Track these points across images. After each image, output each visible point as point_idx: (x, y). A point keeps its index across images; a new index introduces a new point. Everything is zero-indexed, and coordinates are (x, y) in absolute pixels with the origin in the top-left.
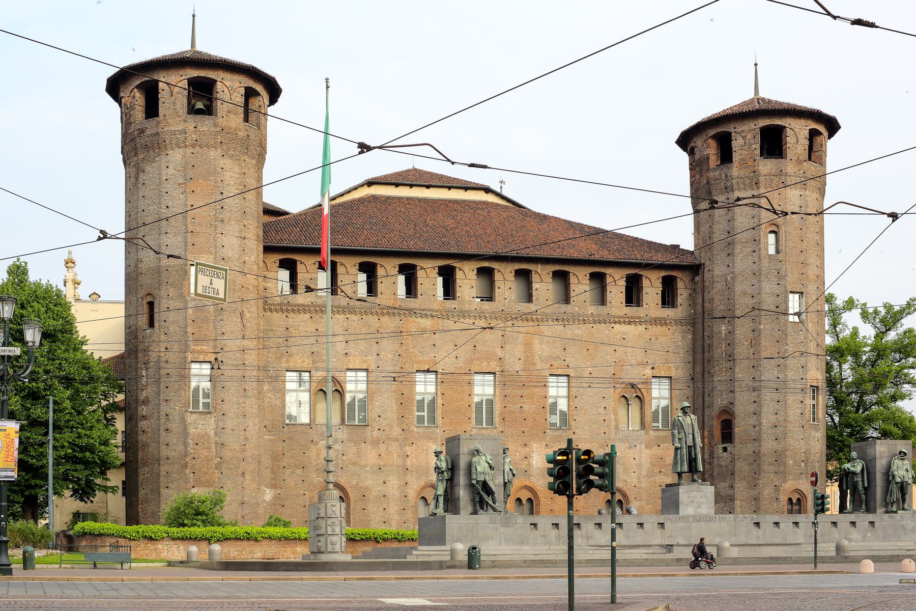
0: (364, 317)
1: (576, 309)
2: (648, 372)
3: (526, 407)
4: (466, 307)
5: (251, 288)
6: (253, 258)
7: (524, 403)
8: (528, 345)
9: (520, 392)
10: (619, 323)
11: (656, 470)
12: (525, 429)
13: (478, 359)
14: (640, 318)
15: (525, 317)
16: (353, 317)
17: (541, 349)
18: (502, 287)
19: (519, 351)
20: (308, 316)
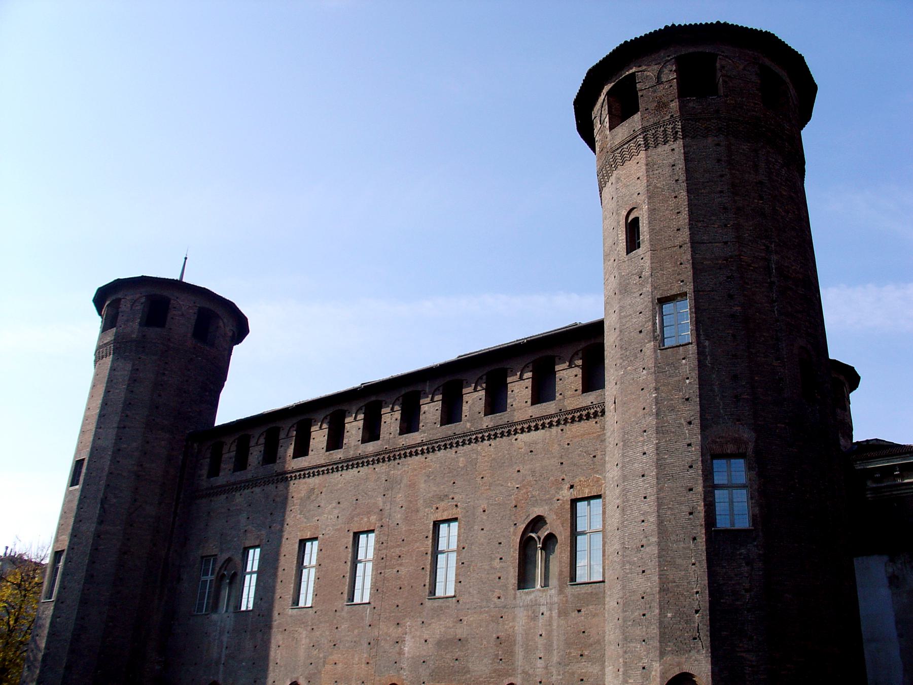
0: (265, 488)
1: (468, 425)
2: (567, 494)
3: (403, 571)
4: (351, 454)
5: (125, 474)
6: (135, 444)
7: (401, 565)
8: (412, 485)
9: (398, 551)
10: (522, 431)
11: (575, 653)
12: (400, 602)
13: (359, 515)
14: (551, 416)
15: (411, 452)
16: (257, 490)
17: (425, 489)
18: (388, 420)
19: (400, 498)
20: (224, 497)
